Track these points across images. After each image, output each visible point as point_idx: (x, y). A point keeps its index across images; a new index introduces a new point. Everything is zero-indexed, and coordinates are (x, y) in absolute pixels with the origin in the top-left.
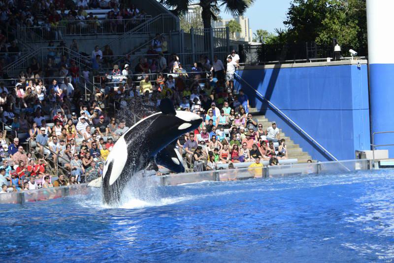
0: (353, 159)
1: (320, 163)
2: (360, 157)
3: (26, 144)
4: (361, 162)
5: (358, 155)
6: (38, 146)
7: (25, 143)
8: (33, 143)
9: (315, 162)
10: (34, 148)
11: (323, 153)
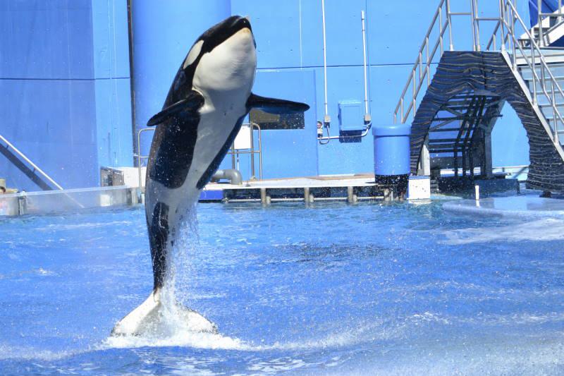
0: (95, 185)
1: (23, 194)
2: (110, 182)
4: (113, 193)
5: (106, 177)
9: (14, 193)
11: (31, 174)
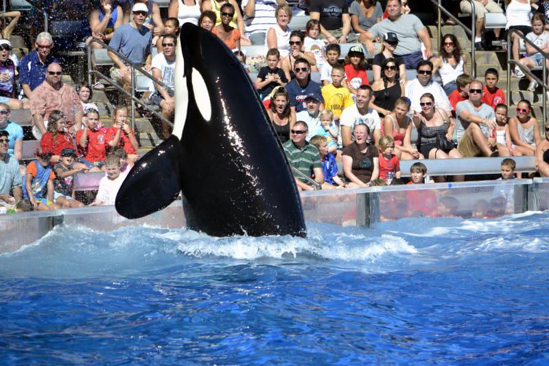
3: (77, 57)
6: (117, 66)
7: (74, 53)
8: (100, 54)
10: (105, 70)
